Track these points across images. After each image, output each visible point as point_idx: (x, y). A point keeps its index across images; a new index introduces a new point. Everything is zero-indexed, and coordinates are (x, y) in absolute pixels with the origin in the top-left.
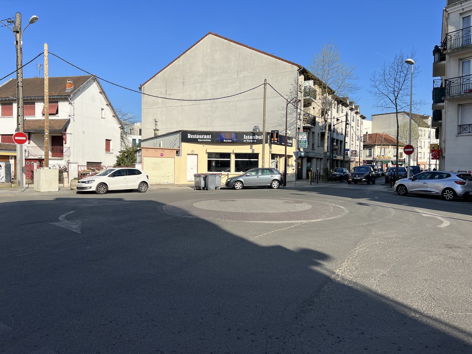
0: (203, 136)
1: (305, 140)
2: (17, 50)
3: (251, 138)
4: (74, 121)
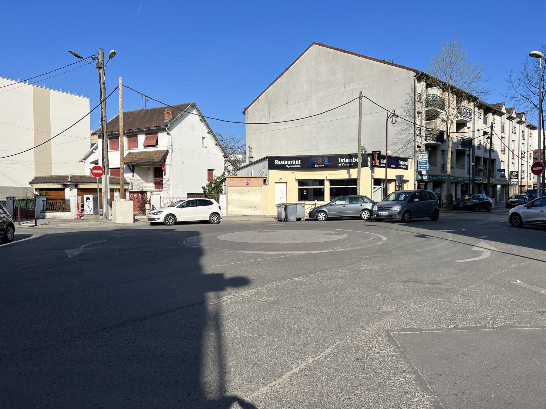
0: (291, 161)
1: (425, 161)
2: (101, 85)
3: (348, 161)
4: (173, 151)
